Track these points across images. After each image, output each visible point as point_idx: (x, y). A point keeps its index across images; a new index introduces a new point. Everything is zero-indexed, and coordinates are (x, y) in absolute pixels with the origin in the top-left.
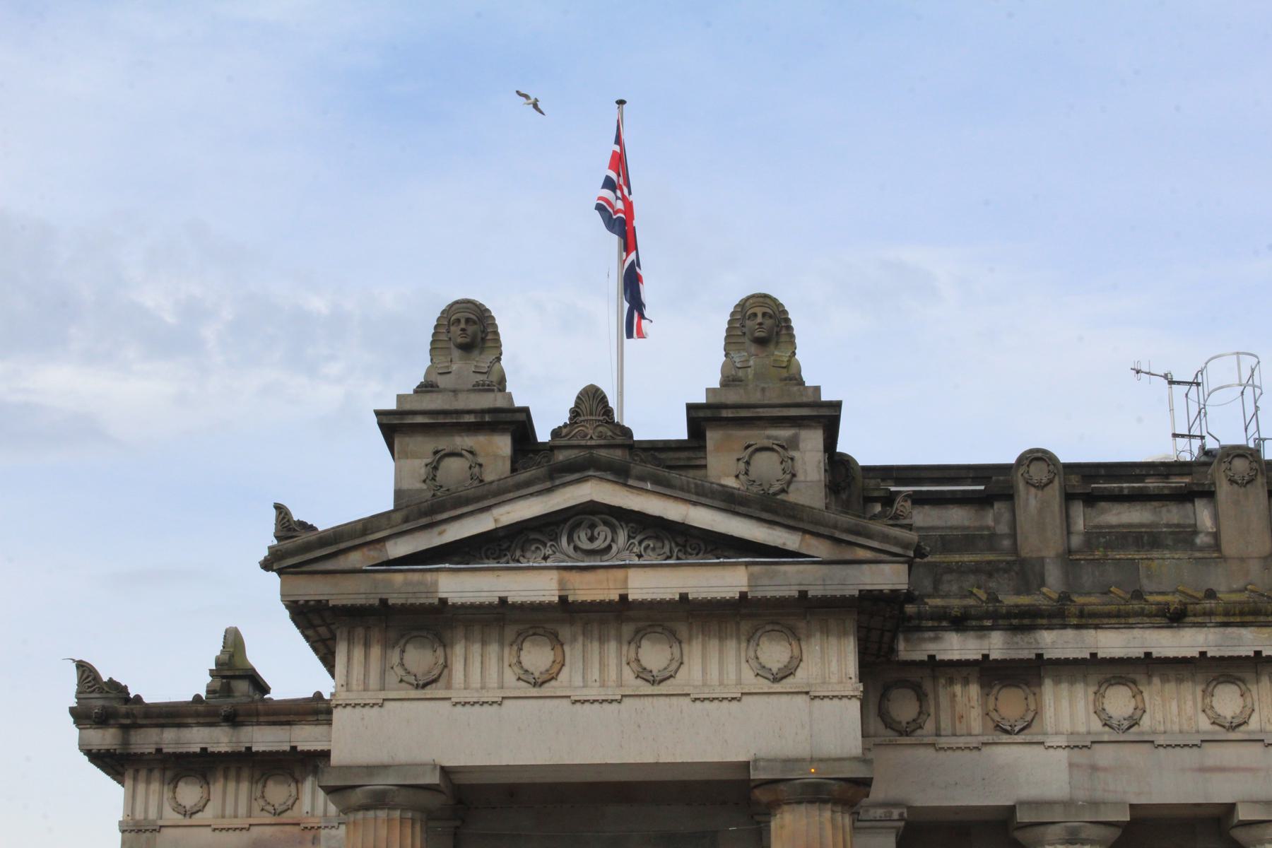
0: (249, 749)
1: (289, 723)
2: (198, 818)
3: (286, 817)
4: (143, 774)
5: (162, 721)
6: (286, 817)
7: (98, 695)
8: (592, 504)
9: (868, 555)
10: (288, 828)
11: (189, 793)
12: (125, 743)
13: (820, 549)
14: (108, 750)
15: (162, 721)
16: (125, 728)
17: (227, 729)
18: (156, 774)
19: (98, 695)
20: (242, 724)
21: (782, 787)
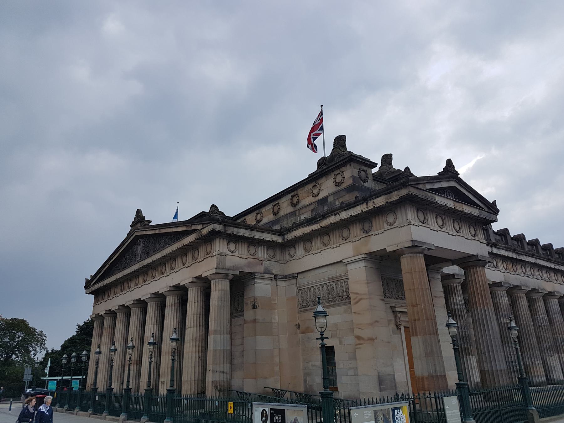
0: (254, 237)
1: (263, 232)
2: (235, 254)
3: (255, 257)
4: (222, 239)
5: (235, 225)
6: (255, 257)
7: (218, 215)
8: (455, 186)
9: (491, 212)
10: (256, 260)
11: (232, 246)
12: (225, 230)
13: (486, 209)
14: (220, 231)
15: (235, 225)
16: (225, 225)
17: (249, 231)
18: (225, 240)
19: (218, 215)
20: (252, 230)
21: (481, 262)
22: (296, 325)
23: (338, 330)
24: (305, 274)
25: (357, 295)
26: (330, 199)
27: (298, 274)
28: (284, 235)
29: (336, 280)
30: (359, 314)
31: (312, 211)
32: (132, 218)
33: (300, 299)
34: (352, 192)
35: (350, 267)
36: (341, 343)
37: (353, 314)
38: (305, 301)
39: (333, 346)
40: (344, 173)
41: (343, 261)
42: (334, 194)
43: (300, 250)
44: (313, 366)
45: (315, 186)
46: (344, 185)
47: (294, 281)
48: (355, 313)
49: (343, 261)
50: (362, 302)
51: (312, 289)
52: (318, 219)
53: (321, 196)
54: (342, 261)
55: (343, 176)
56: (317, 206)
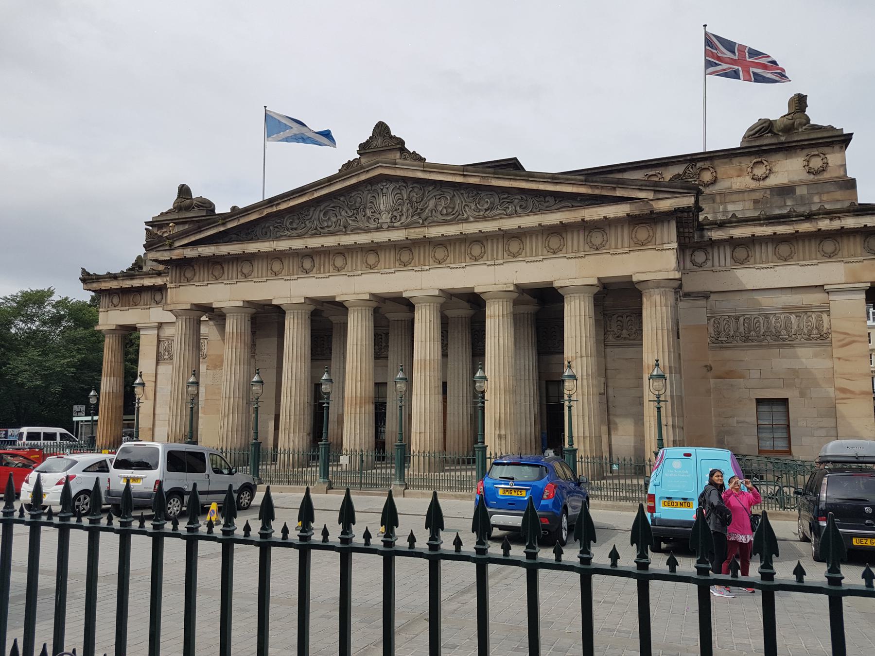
22: (706, 366)
23: (798, 378)
24: (728, 294)
25: (845, 336)
26: (801, 191)
27: (711, 292)
28: (703, 230)
29: (802, 311)
30: (846, 360)
31: (756, 202)
32: (366, 134)
33: (711, 331)
34: (848, 189)
35: (832, 297)
36: (802, 395)
37: (836, 361)
38: (723, 335)
39: (788, 399)
40: (827, 156)
41: (826, 287)
42: (809, 184)
43: (722, 258)
44: (738, 422)
45: (761, 162)
46: (826, 176)
47: (702, 303)
48: (839, 359)
49: (825, 286)
50: (854, 345)
51: (741, 319)
52: (794, 219)
53: (772, 181)
54: (823, 286)
55: (825, 161)
56: (769, 196)
